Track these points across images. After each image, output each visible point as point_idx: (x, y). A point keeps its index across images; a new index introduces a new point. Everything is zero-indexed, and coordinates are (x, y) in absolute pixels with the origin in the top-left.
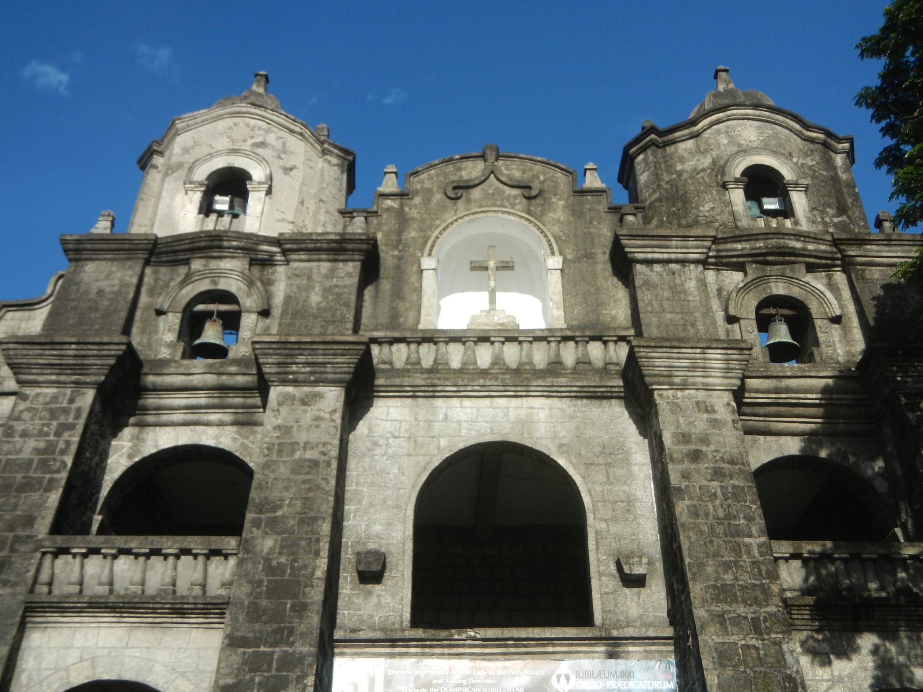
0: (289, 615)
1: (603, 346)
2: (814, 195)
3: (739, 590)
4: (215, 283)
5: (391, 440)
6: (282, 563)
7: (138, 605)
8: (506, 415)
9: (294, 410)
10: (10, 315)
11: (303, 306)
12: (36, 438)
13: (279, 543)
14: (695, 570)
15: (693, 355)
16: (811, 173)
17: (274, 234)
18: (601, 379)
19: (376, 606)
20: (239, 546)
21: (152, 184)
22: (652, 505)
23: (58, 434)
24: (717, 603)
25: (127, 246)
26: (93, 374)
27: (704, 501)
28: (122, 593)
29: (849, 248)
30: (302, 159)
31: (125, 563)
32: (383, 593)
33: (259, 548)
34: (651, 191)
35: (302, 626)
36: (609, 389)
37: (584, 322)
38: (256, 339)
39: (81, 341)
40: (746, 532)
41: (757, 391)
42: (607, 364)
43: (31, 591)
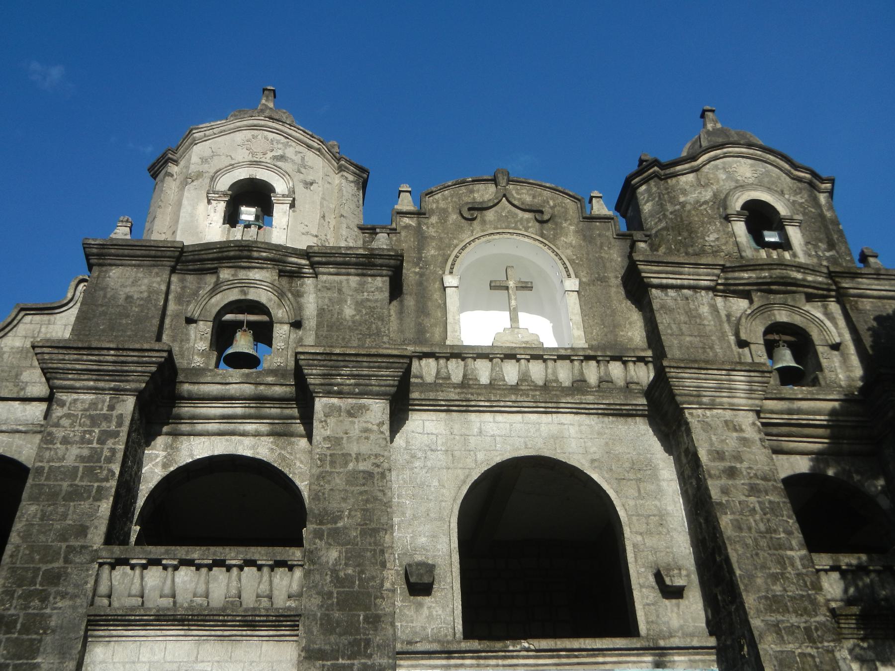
0: (364, 627)
1: (622, 366)
2: (806, 230)
3: (789, 601)
4: (245, 294)
5: (429, 453)
6: (349, 574)
7: (208, 618)
8: (538, 430)
9: (341, 421)
10: (28, 319)
11: (337, 319)
12: (78, 446)
13: (344, 554)
14: (746, 581)
16: (802, 209)
17: (303, 247)
18: (626, 398)
19: (428, 617)
20: (304, 557)
22: (683, 519)
23: (101, 441)
24: (771, 613)
25: (153, 253)
26: (133, 381)
27: (745, 516)
28: (186, 605)
30: (321, 174)
31: (186, 575)
32: (434, 605)
33: (324, 559)
34: (657, 220)
35: (378, 638)
36: (634, 407)
37: (603, 342)
38: (300, 350)
39: (120, 347)
40: (787, 545)
41: (772, 412)
42: (627, 384)
43: (92, 604)
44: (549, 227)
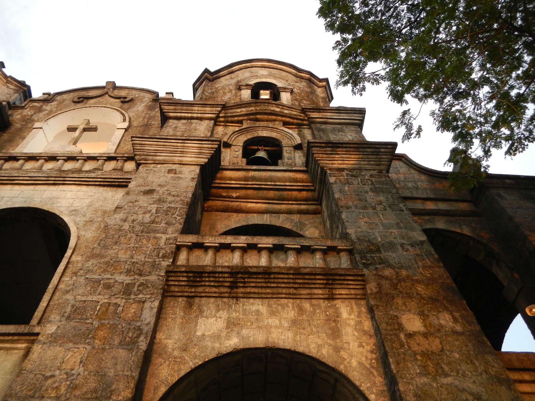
15: (175, 144)
29: (313, 113)
36: (125, 180)
41: (231, 179)
44: (126, 106)
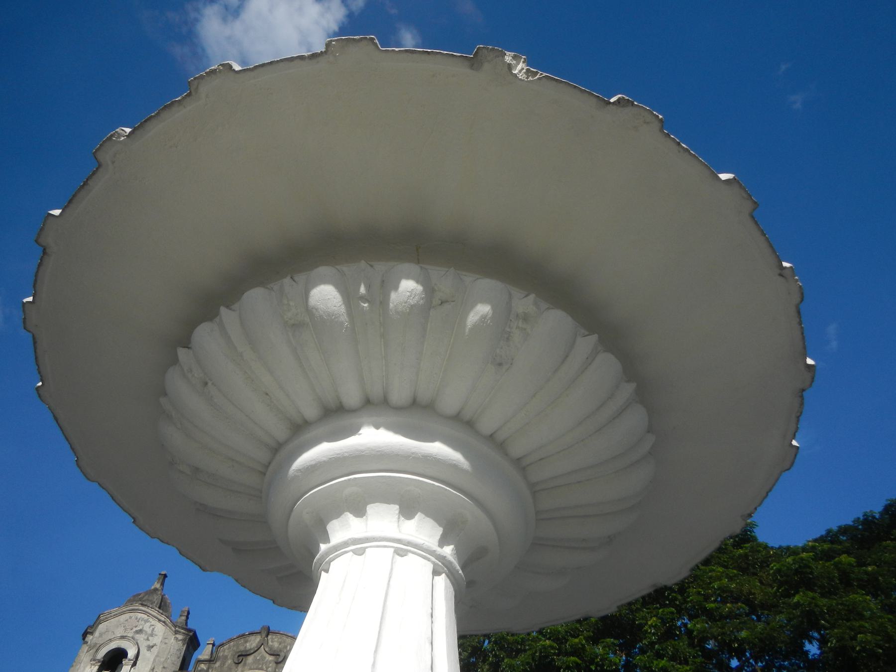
21: (81, 655)
30: (161, 638)
